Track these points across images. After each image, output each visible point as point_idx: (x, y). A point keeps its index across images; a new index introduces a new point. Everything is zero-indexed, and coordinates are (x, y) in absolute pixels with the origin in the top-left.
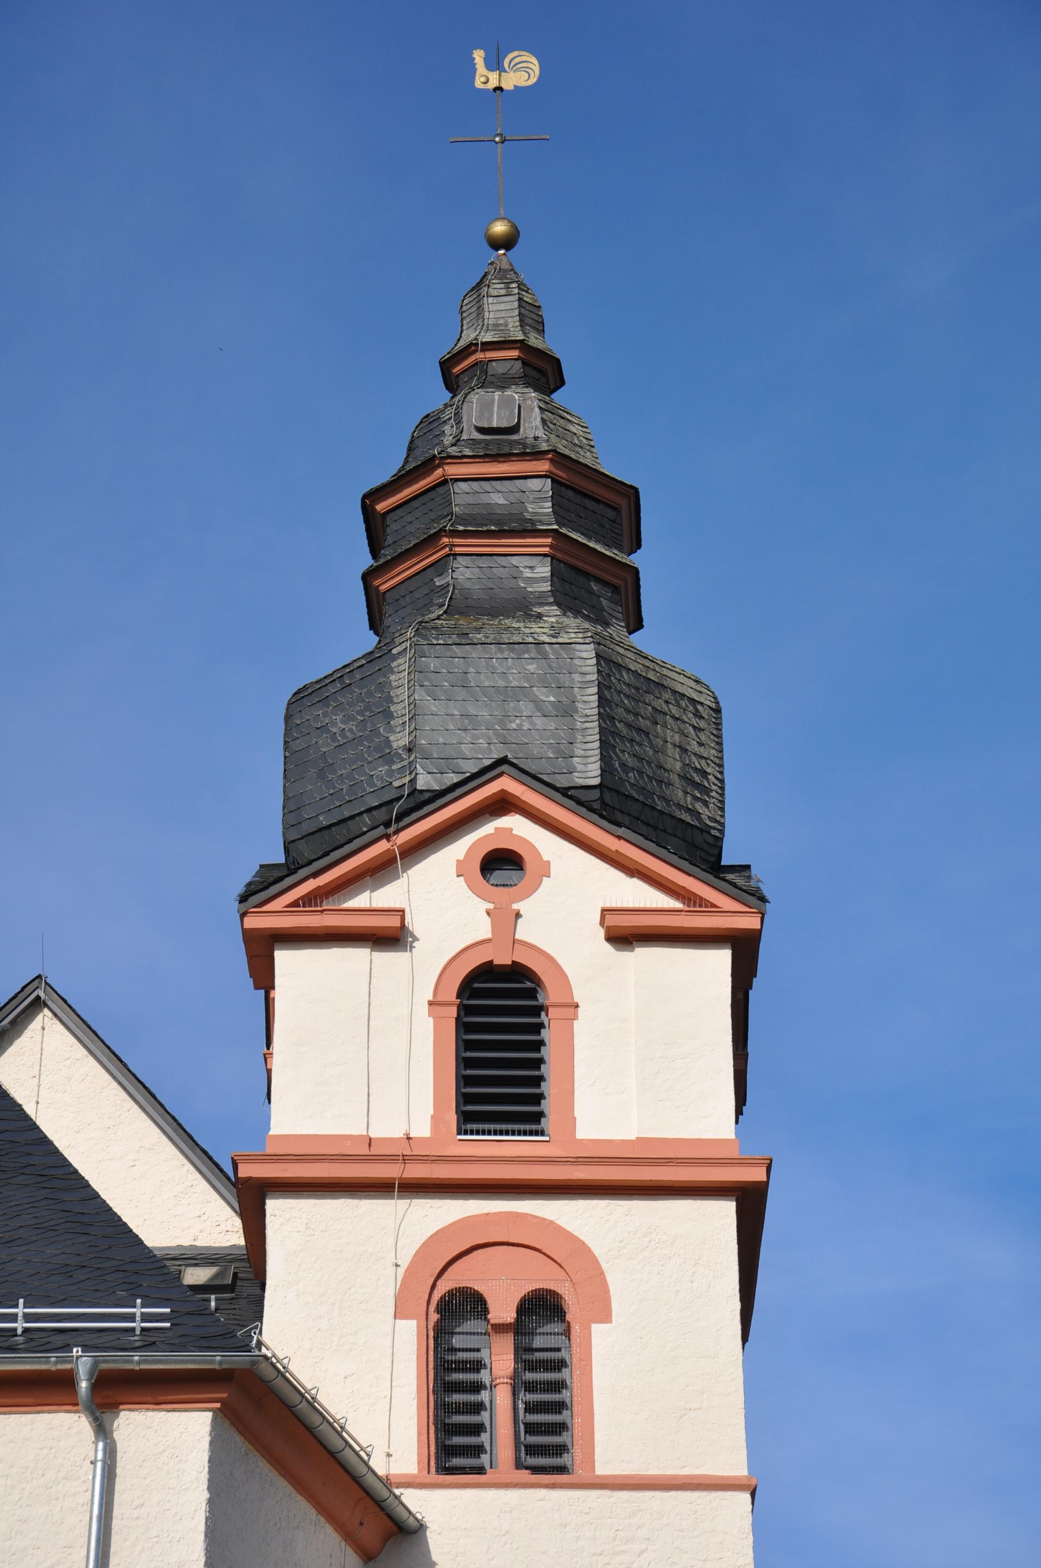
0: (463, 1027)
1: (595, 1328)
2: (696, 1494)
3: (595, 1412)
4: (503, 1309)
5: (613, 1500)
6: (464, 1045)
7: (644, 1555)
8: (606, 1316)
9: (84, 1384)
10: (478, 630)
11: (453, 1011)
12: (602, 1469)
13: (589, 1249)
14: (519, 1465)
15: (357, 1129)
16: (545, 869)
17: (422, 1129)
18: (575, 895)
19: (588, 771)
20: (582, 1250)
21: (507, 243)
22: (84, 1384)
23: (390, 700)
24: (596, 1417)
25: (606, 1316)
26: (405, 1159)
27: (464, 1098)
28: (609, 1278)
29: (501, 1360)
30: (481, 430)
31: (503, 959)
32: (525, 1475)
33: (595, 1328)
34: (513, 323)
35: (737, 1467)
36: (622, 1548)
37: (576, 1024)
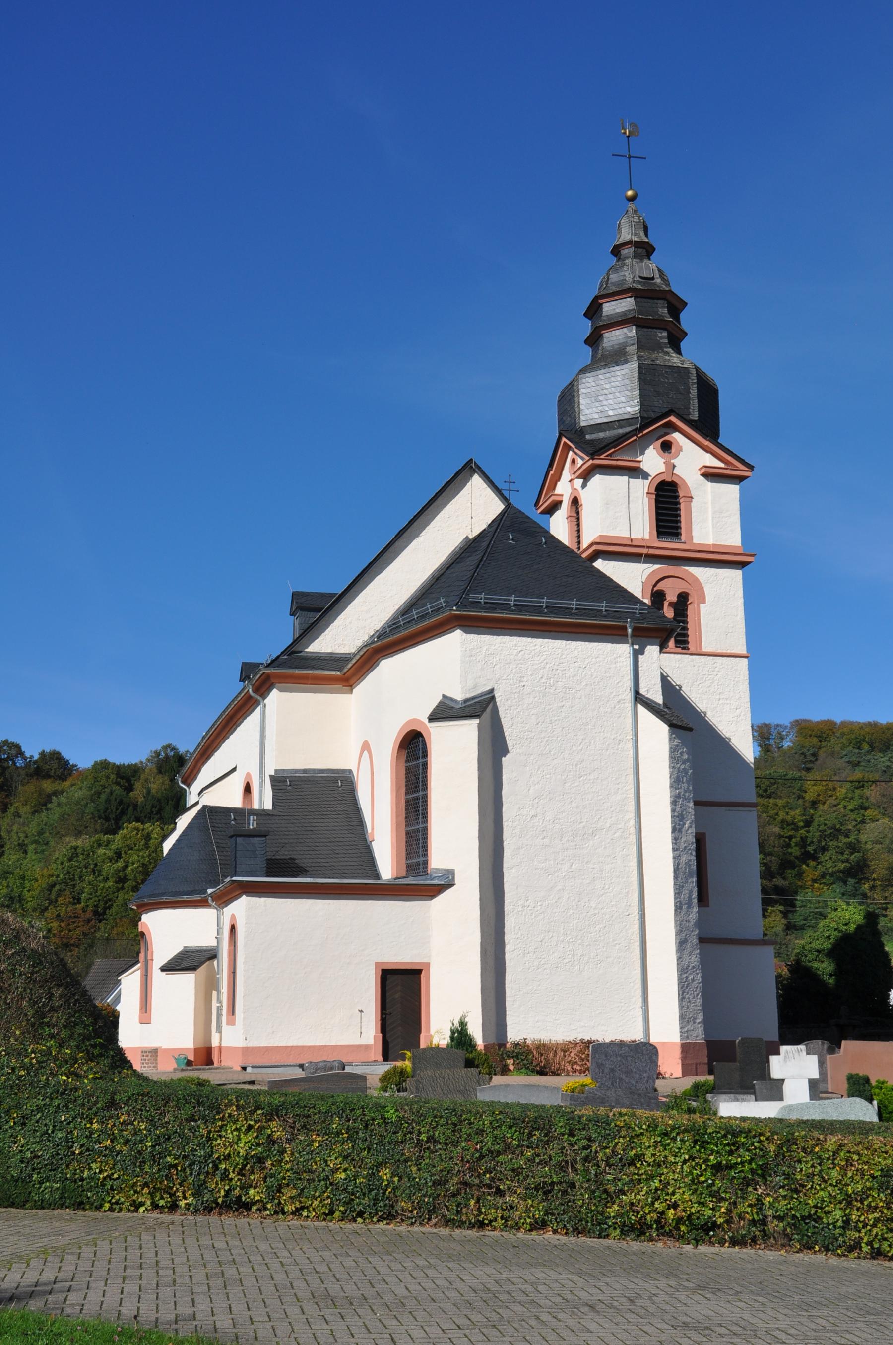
0: (657, 501)
4: (671, 597)
6: (657, 508)
8: (704, 602)
9: (629, 630)
10: (657, 359)
11: (654, 496)
12: (705, 649)
15: (626, 534)
16: (680, 449)
17: (647, 537)
18: (690, 459)
19: (695, 415)
20: (696, 580)
21: (632, 199)
22: (629, 630)
23: (689, 404)
25: (704, 602)
26: (648, 547)
27: (658, 526)
30: (641, 277)
31: (669, 479)
32: (679, 650)
34: (642, 233)
35: (743, 650)
37: (692, 504)
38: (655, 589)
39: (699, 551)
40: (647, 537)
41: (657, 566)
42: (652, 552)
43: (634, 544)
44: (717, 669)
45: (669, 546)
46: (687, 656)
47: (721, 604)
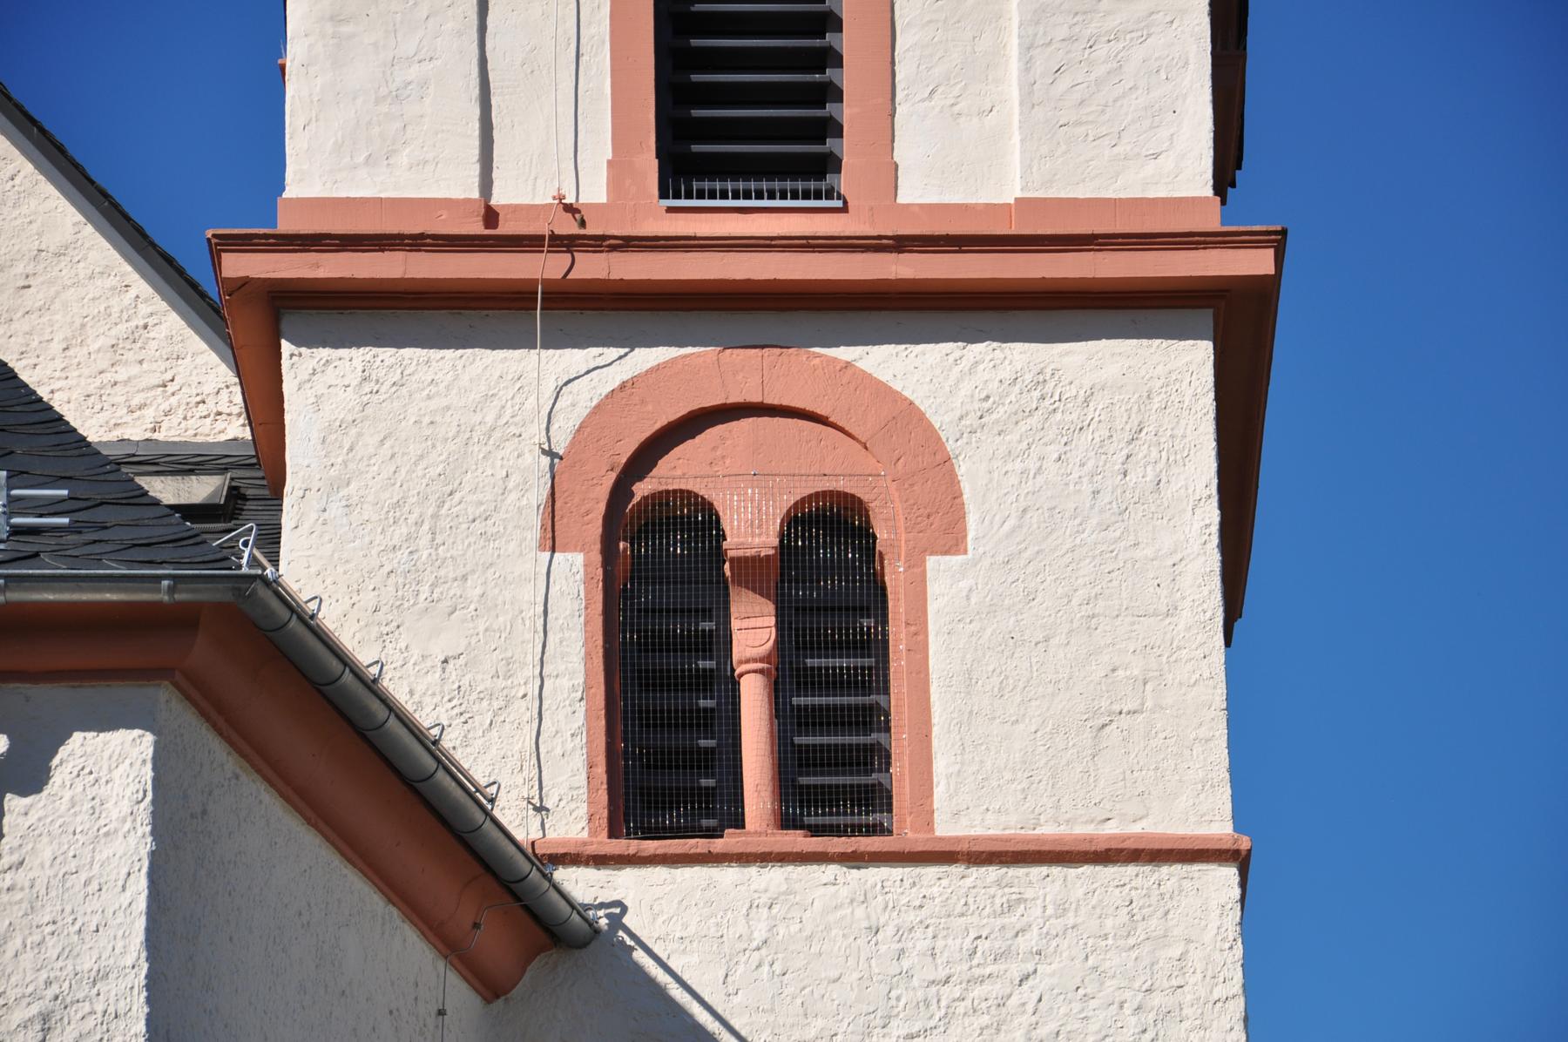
1: (932, 562)
2: (1131, 869)
3: (935, 720)
4: (750, 528)
5: (969, 882)
7: (1031, 982)
13: (921, 417)
14: (786, 822)
20: (906, 418)
24: (935, 731)
25: (953, 540)
28: (962, 469)
29: (753, 630)
32: (797, 840)
33: (932, 562)
35: (1214, 820)
36: (988, 971)
38: (642, 489)
39: (901, 244)
40: (595, 192)
41: (646, 358)
42: (591, 267)
43: (505, 228)
44: (1026, 943)
45: (747, 233)
46: (833, 870)
47: (1066, 553)
